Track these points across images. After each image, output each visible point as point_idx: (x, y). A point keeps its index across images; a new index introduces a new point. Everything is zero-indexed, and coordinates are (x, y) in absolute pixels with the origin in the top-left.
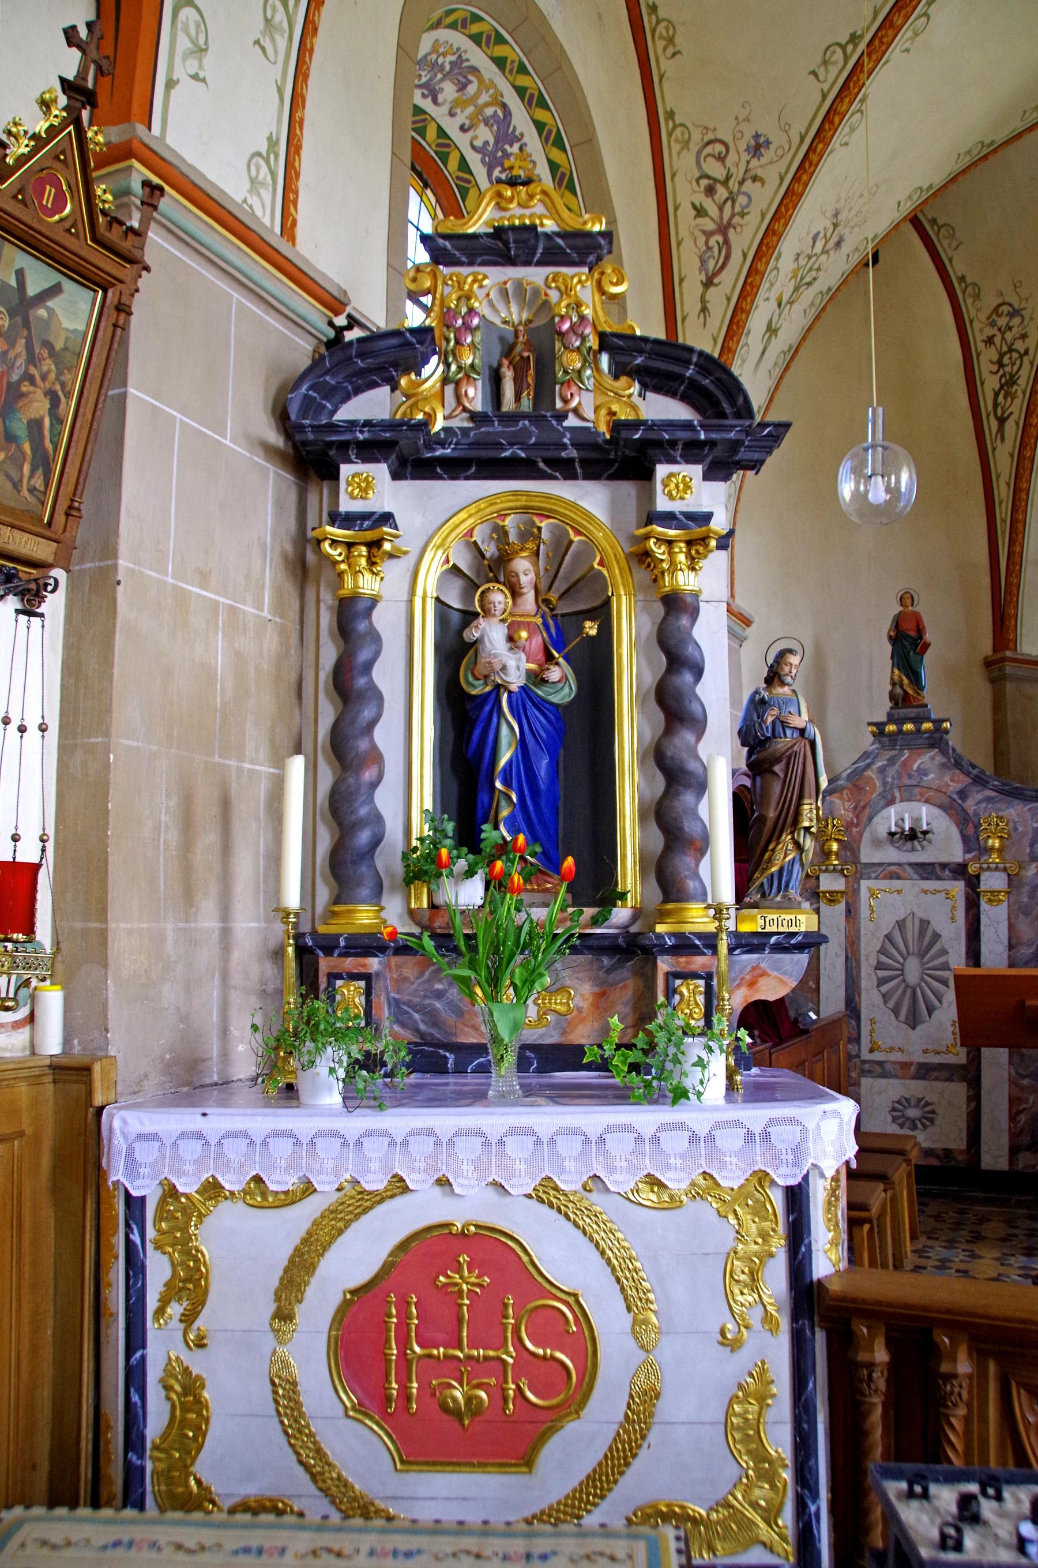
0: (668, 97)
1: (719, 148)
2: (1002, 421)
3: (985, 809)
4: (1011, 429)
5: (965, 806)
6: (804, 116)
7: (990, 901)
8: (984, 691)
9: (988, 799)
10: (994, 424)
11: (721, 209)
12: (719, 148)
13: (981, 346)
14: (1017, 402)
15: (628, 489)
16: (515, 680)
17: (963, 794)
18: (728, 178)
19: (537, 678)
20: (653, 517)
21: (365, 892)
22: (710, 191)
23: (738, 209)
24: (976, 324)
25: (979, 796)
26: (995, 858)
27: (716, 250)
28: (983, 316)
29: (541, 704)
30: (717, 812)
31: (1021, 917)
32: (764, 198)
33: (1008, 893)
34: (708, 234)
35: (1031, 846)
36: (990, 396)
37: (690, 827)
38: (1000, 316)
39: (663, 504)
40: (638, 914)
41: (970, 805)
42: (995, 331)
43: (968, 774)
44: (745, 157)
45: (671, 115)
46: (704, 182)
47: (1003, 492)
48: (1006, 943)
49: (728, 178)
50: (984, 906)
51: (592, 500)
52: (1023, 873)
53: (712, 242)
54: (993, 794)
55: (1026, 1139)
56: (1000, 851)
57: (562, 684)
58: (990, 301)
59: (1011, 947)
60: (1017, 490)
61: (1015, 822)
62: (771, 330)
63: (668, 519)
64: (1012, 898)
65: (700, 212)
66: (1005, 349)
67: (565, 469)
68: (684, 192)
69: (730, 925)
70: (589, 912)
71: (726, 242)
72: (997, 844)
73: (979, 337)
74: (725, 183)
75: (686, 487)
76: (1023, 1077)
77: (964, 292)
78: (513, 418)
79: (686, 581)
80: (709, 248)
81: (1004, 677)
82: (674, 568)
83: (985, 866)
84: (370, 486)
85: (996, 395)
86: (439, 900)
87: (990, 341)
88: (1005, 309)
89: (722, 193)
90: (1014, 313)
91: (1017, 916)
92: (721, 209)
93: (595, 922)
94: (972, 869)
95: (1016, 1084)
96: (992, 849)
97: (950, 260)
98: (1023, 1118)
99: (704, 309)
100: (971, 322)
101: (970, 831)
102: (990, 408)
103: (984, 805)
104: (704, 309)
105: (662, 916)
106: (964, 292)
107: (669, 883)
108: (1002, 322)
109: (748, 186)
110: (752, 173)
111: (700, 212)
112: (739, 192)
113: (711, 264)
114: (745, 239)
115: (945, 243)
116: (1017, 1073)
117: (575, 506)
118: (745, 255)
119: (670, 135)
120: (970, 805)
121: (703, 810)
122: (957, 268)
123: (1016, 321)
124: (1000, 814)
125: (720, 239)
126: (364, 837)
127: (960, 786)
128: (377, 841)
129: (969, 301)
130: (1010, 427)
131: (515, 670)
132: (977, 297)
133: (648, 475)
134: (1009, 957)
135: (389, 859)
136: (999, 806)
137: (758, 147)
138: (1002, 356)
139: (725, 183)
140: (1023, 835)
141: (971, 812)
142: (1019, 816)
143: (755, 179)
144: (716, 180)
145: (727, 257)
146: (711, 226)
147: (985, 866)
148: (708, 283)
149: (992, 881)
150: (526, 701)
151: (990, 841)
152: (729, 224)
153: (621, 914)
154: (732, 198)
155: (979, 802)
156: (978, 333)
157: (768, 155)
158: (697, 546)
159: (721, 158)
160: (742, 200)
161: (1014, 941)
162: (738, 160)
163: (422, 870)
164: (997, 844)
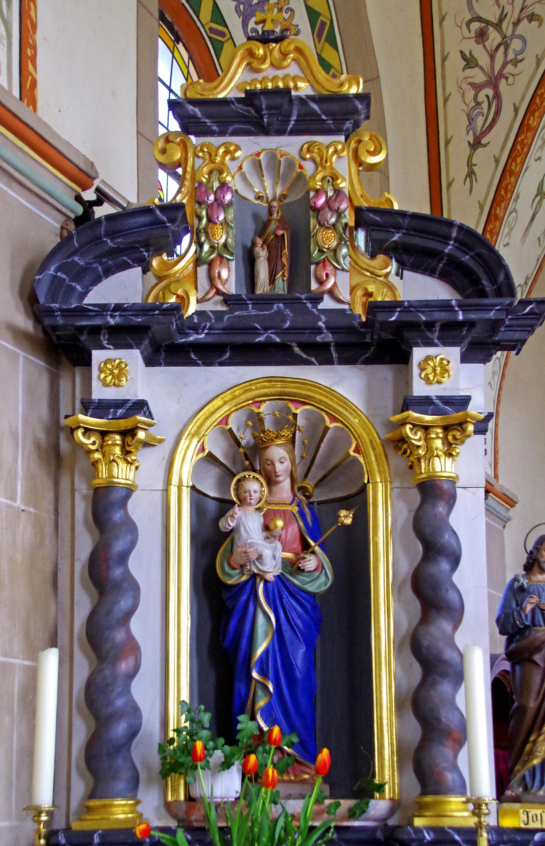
11: (492, 57)
15: (384, 373)
16: (271, 569)
18: (501, 19)
19: (293, 567)
20: (409, 403)
21: (121, 785)
22: (481, 36)
23: (511, 56)
27: (485, 106)
29: (297, 593)
30: (476, 702)
34: (477, 88)
37: (447, 717)
39: (420, 389)
40: (396, 805)
46: (476, 26)
49: (501, 19)
51: (347, 385)
53: (481, 97)
57: (318, 573)
63: (424, 404)
65: (470, 62)
67: (320, 354)
68: (453, 39)
69: (491, 820)
70: (346, 804)
71: (497, 95)
74: (498, 26)
75: (443, 370)
78: (267, 301)
79: (443, 467)
80: (478, 104)
82: (430, 454)
84: (123, 372)
86: (195, 793)
89: (494, 37)
92: (492, 57)
93: (352, 814)
99: (471, 174)
104: (471, 174)
105: (421, 809)
107: (428, 773)
109: (524, 27)
110: (527, 12)
111: (470, 62)
112: (513, 36)
113: (480, 121)
117: (330, 392)
118: (516, 110)
121: (460, 700)
125: (490, 92)
126: (120, 729)
128: (134, 732)
131: (271, 559)
133: (404, 359)
135: (145, 752)
139: (498, 26)
143: (532, 18)
144: (488, 23)
145: (498, 113)
146: (480, 78)
148: (476, 145)
150: (282, 590)
152: (501, 75)
153: (379, 806)
154: (505, 44)
158: (454, 431)
160: (516, 44)
163: (178, 762)
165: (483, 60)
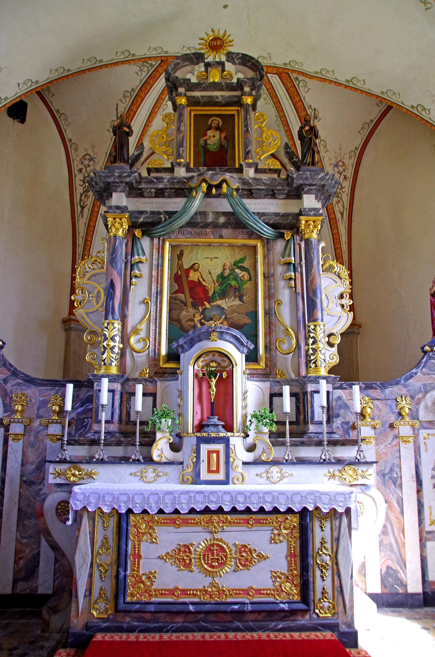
2: (83, 208)
3: (16, 389)
4: (86, 212)
5: (6, 387)
7: (14, 439)
8: (61, 335)
9: (18, 384)
10: (79, 209)
13: (77, 172)
14: (90, 199)
17: (5, 381)
24: (75, 161)
25: (14, 382)
26: (18, 416)
28: (78, 159)
31: (29, 448)
33: (24, 435)
35: (38, 410)
36: (79, 196)
38: (85, 160)
41: (9, 387)
42: (82, 166)
43: (9, 370)
47: (80, 241)
48: (20, 463)
50: (10, 442)
52: (32, 424)
54: (21, 381)
55: (23, 574)
56: (22, 412)
59: (23, 465)
60: (86, 240)
61: (30, 397)
64: (26, 437)
66: (86, 175)
72: (20, 408)
73: (77, 168)
76: (23, 538)
77: (71, 147)
81: (71, 328)
83: (12, 420)
85: (81, 195)
87: (80, 171)
88: (88, 157)
90: (91, 159)
91: (28, 448)
94: (5, 422)
95: (20, 543)
96: (17, 411)
97: (65, 131)
98: (22, 562)
100: (73, 161)
101: (8, 401)
102: (78, 201)
103: (16, 387)
106: (71, 147)
108: (86, 162)
115: (63, 122)
116: (21, 536)
120: (9, 387)
122: (68, 135)
123: (92, 163)
124: (24, 392)
127: (4, 376)
129: (73, 151)
130: (86, 210)
132: (76, 150)
134: (21, 470)
136: (23, 387)
138: (85, 178)
140: (34, 404)
141: (9, 391)
142: (33, 393)
147: (12, 420)
149: (16, 429)
151: (17, 407)
155: (14, 385)
156: (76, 166)
161: (24, 461)
164: (20, 408)
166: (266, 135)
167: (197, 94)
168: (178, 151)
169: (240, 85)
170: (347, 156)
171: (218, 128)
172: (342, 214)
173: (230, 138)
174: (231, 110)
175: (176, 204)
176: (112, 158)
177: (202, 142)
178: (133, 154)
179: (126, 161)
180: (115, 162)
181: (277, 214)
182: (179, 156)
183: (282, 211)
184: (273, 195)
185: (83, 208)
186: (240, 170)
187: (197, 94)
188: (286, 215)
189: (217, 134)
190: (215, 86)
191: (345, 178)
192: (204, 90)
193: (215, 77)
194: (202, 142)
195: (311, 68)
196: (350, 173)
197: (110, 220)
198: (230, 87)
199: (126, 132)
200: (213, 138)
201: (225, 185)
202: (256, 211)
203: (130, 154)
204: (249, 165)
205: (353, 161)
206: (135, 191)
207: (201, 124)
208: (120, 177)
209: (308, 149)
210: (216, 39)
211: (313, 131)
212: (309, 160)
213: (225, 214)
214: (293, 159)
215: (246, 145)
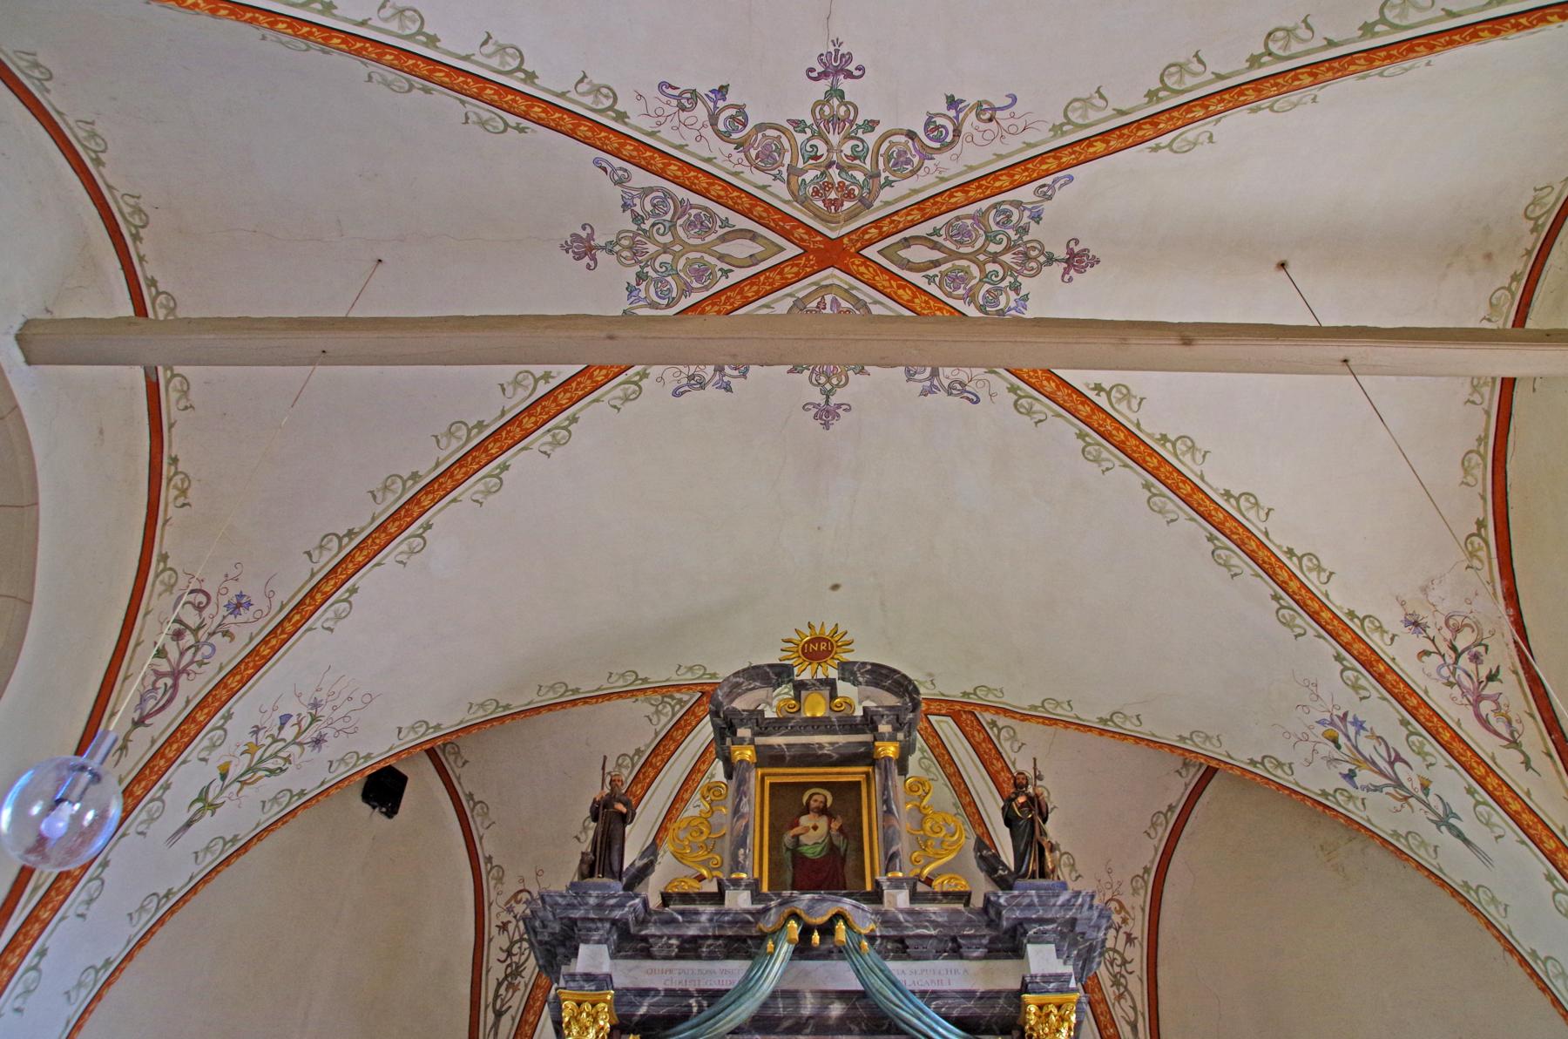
0: (166, 540)
1: (201, 598)
2: (499, 1014)
6: (291, 587)
10: (491, 1016)
11: (182, 654)
12: (203, 599)
13: (495, 931)
14: (518, 994)
18: (199, 628)
22: (178, 635)
23: (198, 657)
24: (494, 907)
27: (161, 692)
28: (502, 900)
32: (229, 653)
34: (159, 675)
36: (493, 985)
38: (518, 902)
42: (510, 917)
44: (223, 611)
45: (164, 558)
46: (177, 626)
49: (199, 628)
53: (160, 684)
58: (511, 887)
62: (205, 802)
65: (161, 653)
66: (517, 937)
68: (153, 630)
71: (175, 686)
73: (496, 922)
74: (195, 632)
77: (488, 873)
80: (155, 689)
85: (500, 984)
87: (503, 927)
88: (525, 896)
89: (189, 639)
92: (182, 654)
97: (481, 838)
100: (490, 905)
102: (490, 999)
106: (488, 873)
110: (225, 628)
111: (161, 653)
112: (205, 643)
113: (151, 703)
114: (193, 688)
115: (478, 820)
118: (188, 702)
119: (157, 576)
122: (485, 848)
125: (169, 681)
129: (492, 883)
130: (506, 1021)
132: (500, 880)
137: (237, 606)
138: (513, 943)
139: (195, 632)
143: (226, 633)
144: (187, 627)
145: (170, 701)
146: (164, 666)
152: (184, 670)
154: (197, 647)
157: (246, 614)
159: (199, 608)
160: (206, 650)
162: (215, 613)
165: (173, 653)
166: (930, 828)
167: (777, 740)
168: (734, 856)
169: (869, 722)
170: (1127, 888)
171: (823, 811)
172: (1134, 1027)
173: (853, 831)
174: (854, 773)
175: (725, 973)
176: (585, 867)
177: (788, 838)
178: (632, 864)
179: (619, 875)
180: (591, 875)
181: (968, 995)
182: (737, 866)
183: (980, 987)
184: (954, 949)
185: (499, 1014)
186: (876, 896)
187: (777, 740)
188: (990, 996)
189: (823, 822)
190: (816, 725)
191: (1130, 939)
192: (793, 732)
193: (816, 706)
194: (788, 838)
195: (1021, 700)
196: (1139, 927)
197: (569, 1005)
198: (849, 726)
199: (621, 813)
200: (813, 833)
201: (841, 926)
202: (917, 988)
203: (626, 865)
204: (897, 884)
205: (1143, 899)
206: (631, 943)
207: (787, 804)
208: (600, 906)
209: (1029, 843)
210: (816, 640)
211: (1038, 807)
212: (1033, 866)
213: (843, 995)
214: (996, 871)
215: (888, 841)
